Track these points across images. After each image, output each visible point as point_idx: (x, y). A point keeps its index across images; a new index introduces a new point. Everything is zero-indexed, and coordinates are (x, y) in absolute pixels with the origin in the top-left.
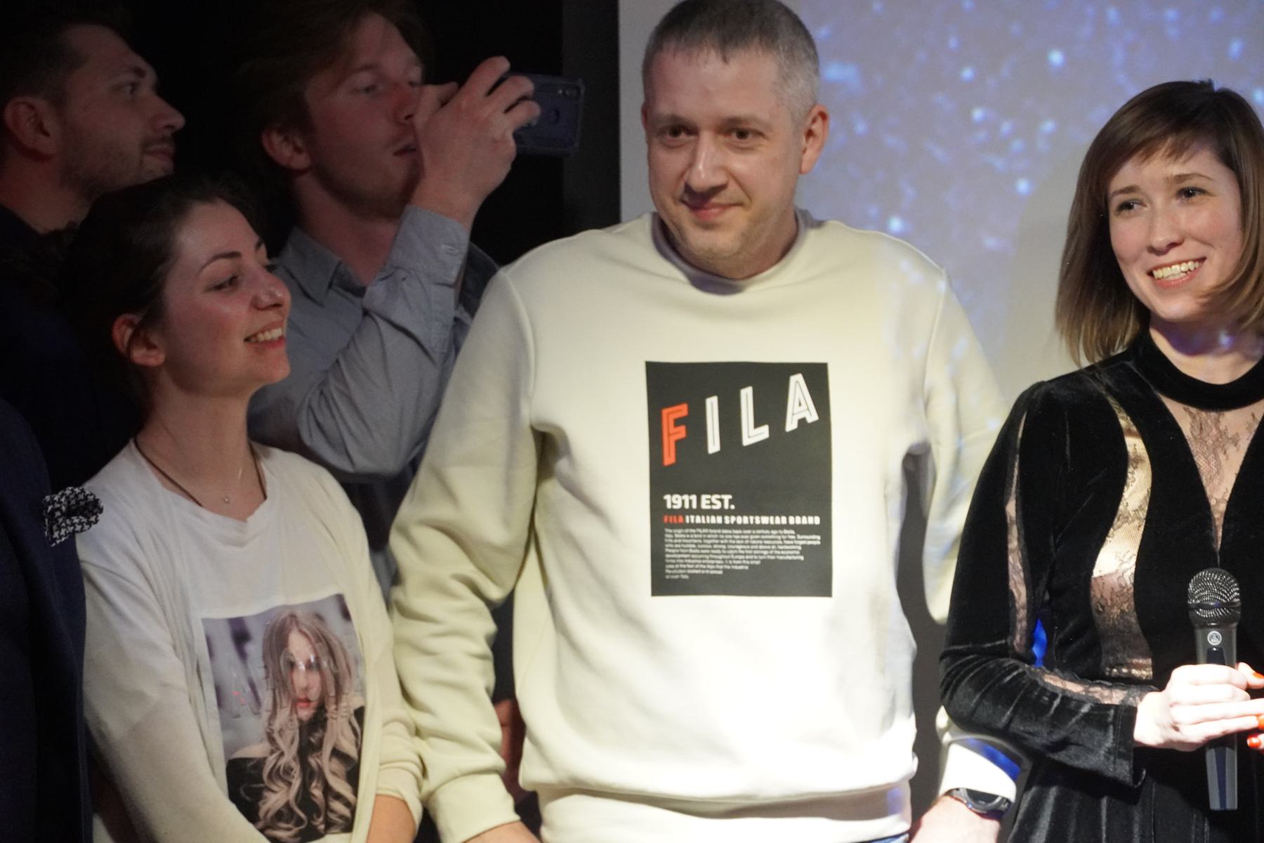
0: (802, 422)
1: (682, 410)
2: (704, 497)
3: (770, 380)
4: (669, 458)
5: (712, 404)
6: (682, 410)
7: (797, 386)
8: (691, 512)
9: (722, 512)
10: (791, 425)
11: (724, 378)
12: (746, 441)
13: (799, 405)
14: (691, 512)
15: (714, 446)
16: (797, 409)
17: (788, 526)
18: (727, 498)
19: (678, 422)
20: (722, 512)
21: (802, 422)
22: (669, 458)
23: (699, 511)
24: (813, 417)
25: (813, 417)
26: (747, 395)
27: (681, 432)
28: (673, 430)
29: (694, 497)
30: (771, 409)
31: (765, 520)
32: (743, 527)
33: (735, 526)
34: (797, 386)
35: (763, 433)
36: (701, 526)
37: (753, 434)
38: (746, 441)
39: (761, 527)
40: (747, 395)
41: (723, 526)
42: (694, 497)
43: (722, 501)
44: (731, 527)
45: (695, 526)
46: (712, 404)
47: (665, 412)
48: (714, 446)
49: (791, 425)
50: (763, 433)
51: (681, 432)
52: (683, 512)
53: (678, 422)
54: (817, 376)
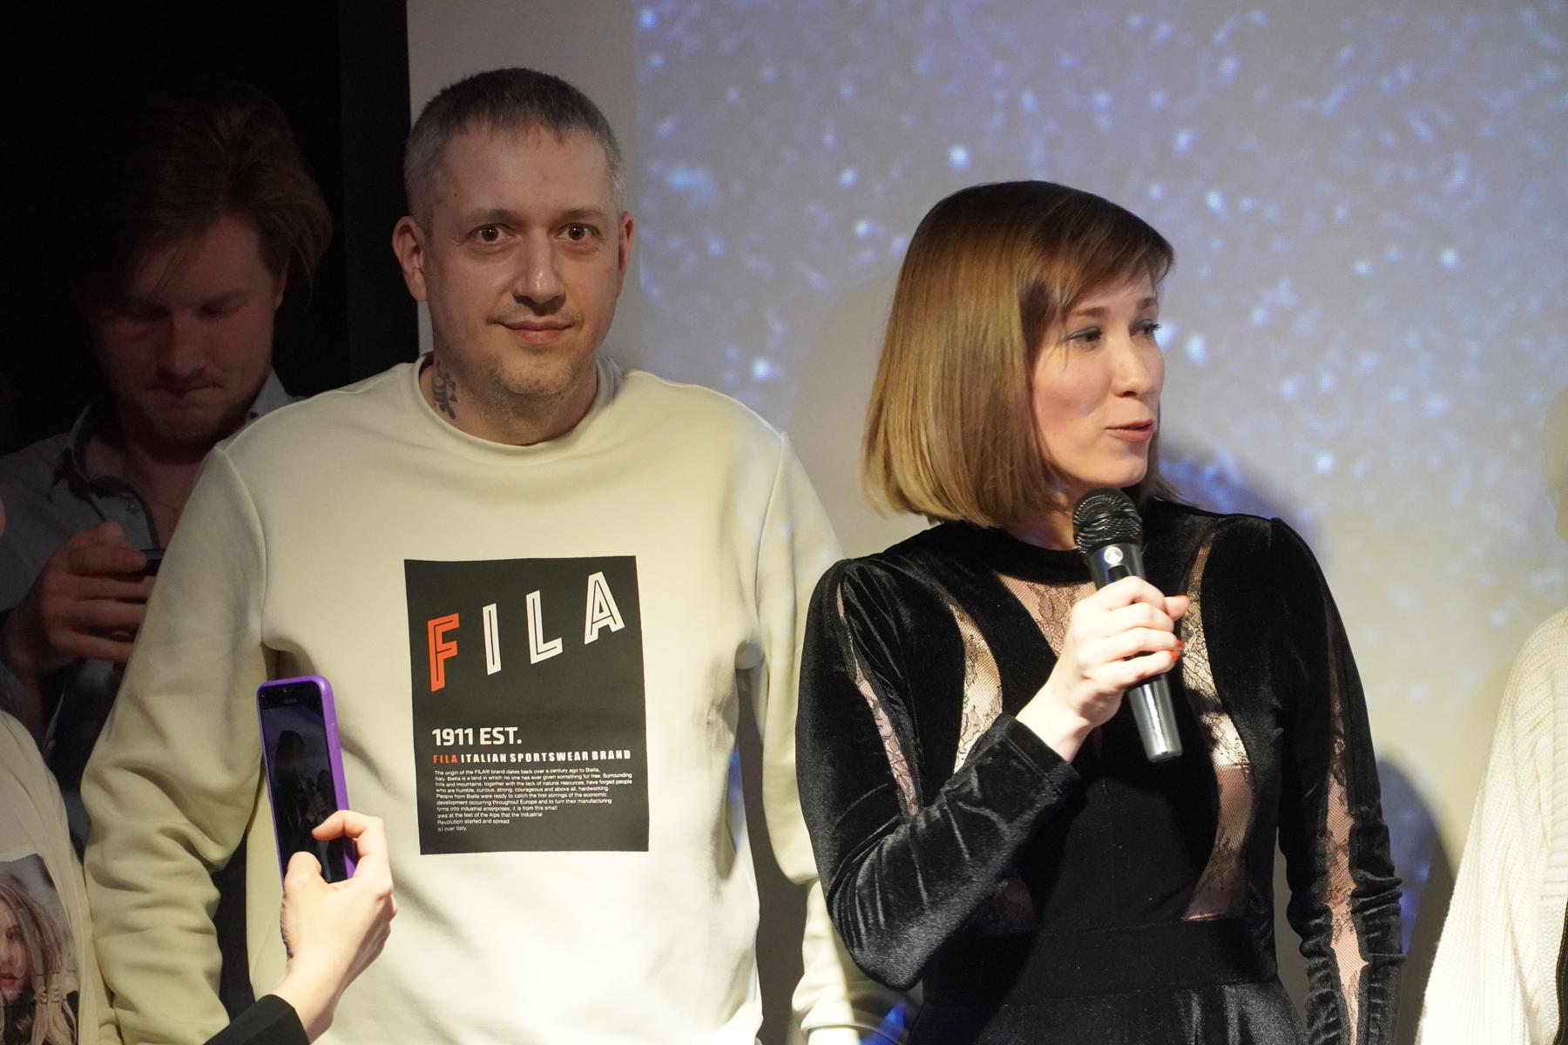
0: (604, 631)
1: (453, 622)
2: (482, 730)
3: (562, 581)
4: (438, 683)
5: (490, 612)
6: (453, 622)
7: (598, 588)
8: (467, 749)
9: (506, 749)
10: (591, 636)
11: (505, 580)
12: (535, 659)
13: (600, 611)
14: (467, 749)
15: (494, 666)
16: (598, 616)
17: (590, 763)
18: (511, 730)
19: (447, 637)
20: (506, 749)
21: (604, 631)
22: (438, 683)
23: (477, 748)
24: (617, 625)
25: (617, 625)
26: (534, 600)
27: (452, 649)
28: (441, 646)
29: (470, 731)
30: (565, 616)
31: (561, 757)
32: (533, 765)
33: (523, 765)
34: (598, 588)
35: (556, 647)
36: (480, 766)
37: (543, 650)
38: (535, 659)
39: (557, 764)
40: (534, 600)
41: (508, 765)
42: (470, 731)
43: (506, 734)
44: (517, 766)
45: (473, 766)
46: (490, 612)
47: (431, 624)
48: (494, 666)
49: (591, 636)
50: (556, 647)
51: (452, 649)
52: (456, 749)
53: (447, 637)
54: (622, 573)
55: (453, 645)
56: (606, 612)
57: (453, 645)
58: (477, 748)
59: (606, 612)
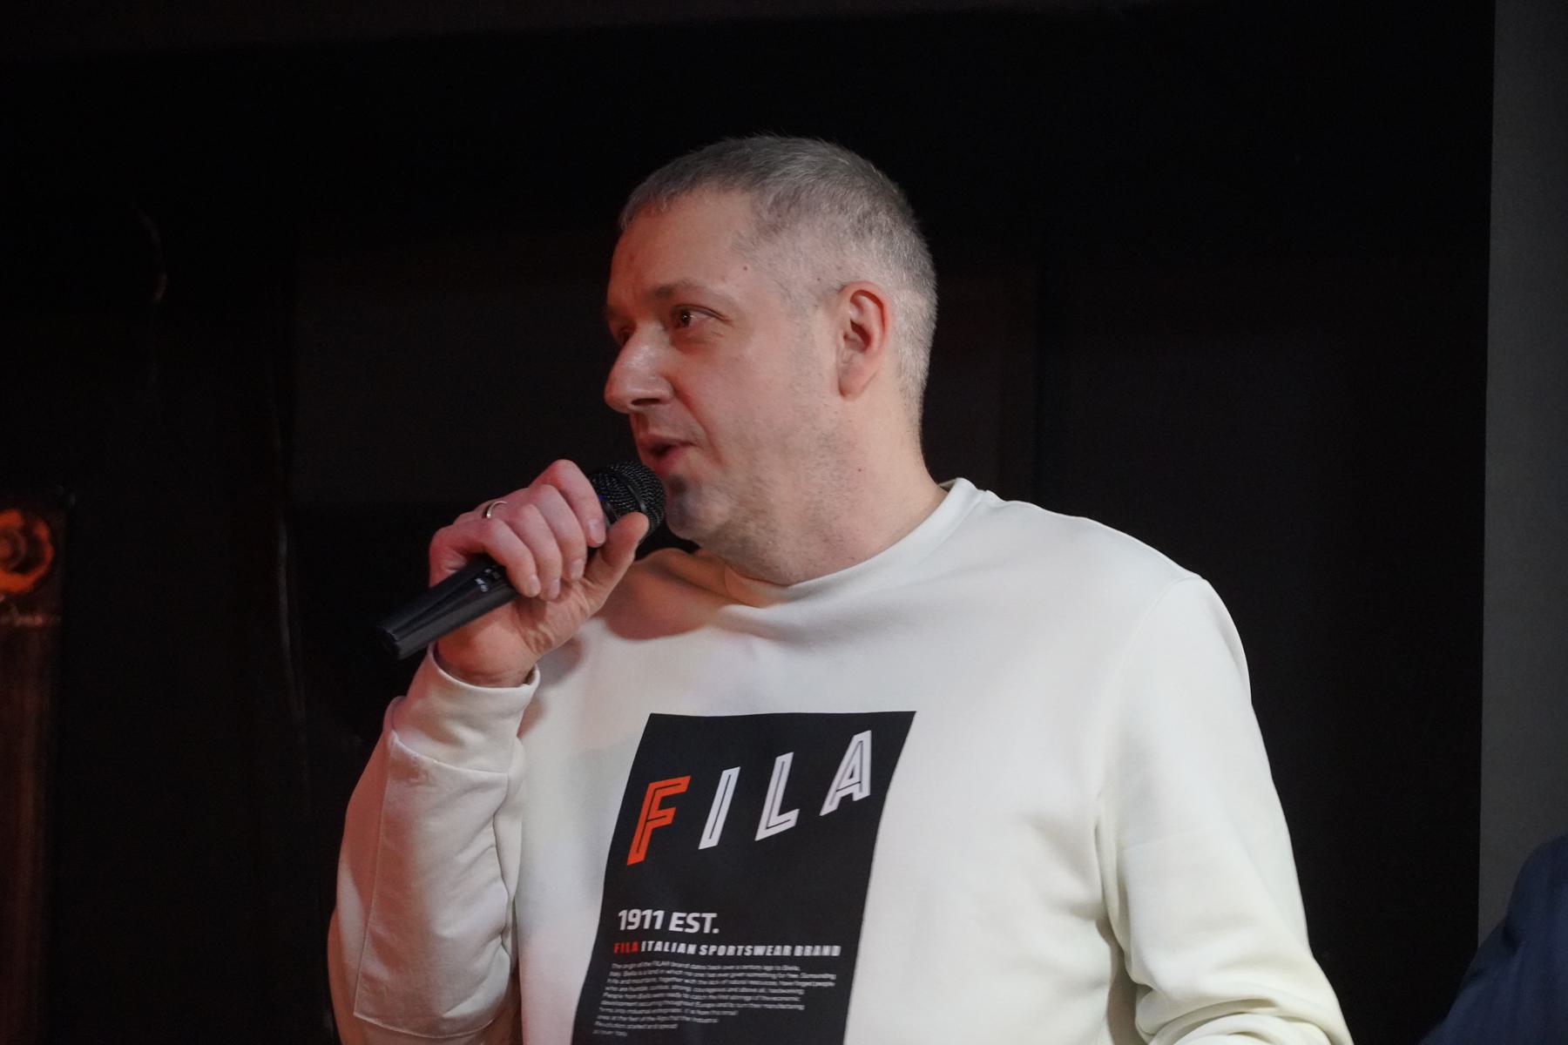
1: (681, 784)
2: (676, 915)
3: (817, 738)
6: (681, 784)
9: (699, 938)
10: (830, 806)
11: (752, 739)
13: (852, 776)
14: (652, 934)
18: (709, 917)
19: (666, 802)
20: (699, 938)
23: (665, 934)
28: (655, 813)
31: (759, 951)
42: (660, 914)
43: (702, 921)
48: (710, 838)
53: (666, 802)
55: (671, 812)
56: (856, 779)
57: (671, 812)
58: (665, 934)
59: (856, 779)
